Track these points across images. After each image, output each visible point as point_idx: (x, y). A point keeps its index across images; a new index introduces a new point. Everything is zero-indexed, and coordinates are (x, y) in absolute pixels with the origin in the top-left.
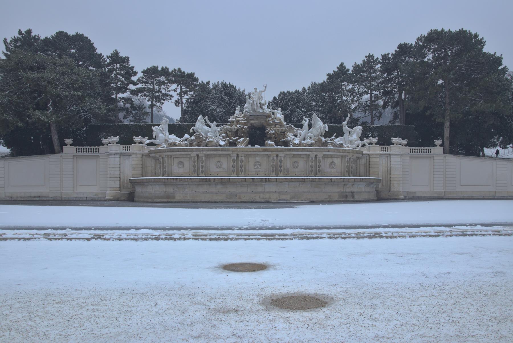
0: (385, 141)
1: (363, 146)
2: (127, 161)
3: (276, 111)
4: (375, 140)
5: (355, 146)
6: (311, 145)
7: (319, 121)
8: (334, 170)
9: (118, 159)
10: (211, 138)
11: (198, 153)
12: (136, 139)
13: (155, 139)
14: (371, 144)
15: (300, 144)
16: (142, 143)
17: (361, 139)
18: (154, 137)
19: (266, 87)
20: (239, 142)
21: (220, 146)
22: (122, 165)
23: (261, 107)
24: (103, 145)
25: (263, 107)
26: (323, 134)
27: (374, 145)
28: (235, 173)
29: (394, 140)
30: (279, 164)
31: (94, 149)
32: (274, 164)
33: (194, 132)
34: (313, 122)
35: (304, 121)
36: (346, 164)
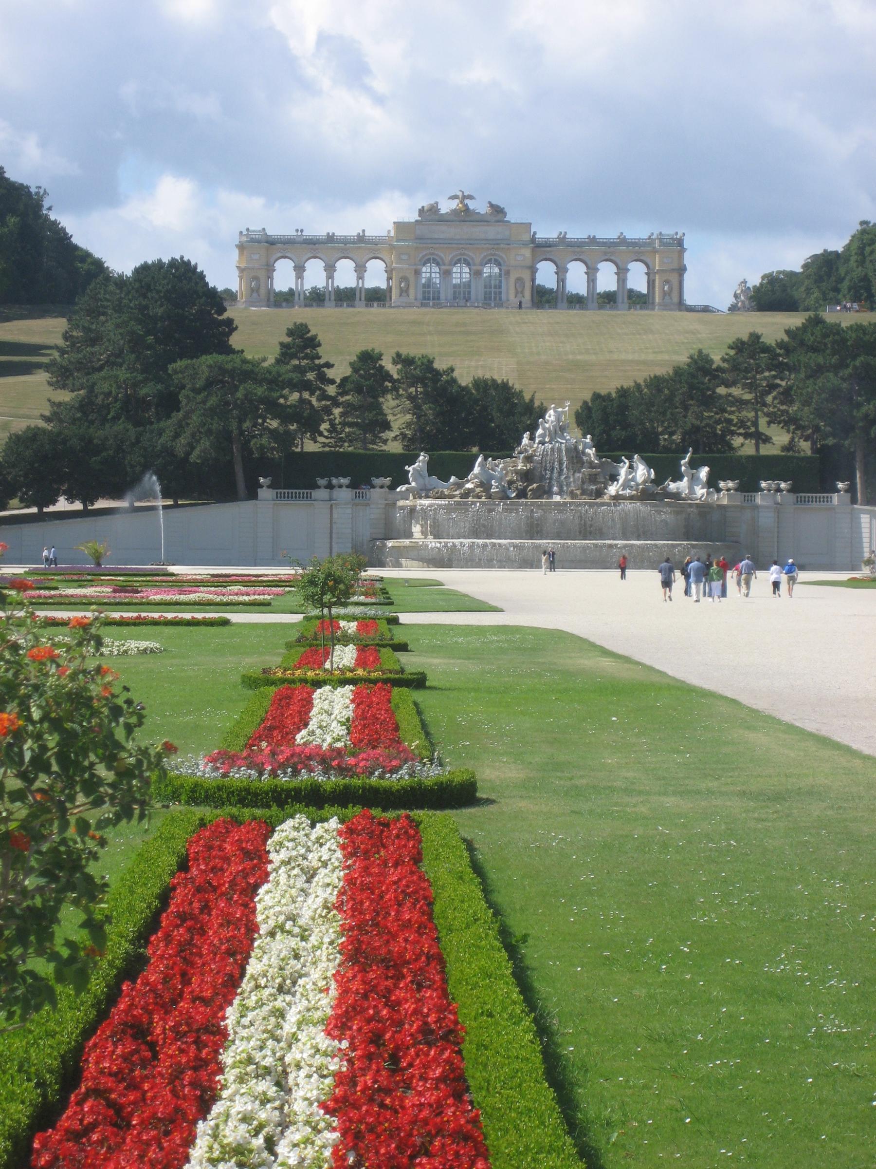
0: (749, 487)
6: (631, 498)
9: (349, 511)
12: (377, 481)
17: (712, 483)
20: (530, 490)
24: (319, 487)
29: (763, 484)
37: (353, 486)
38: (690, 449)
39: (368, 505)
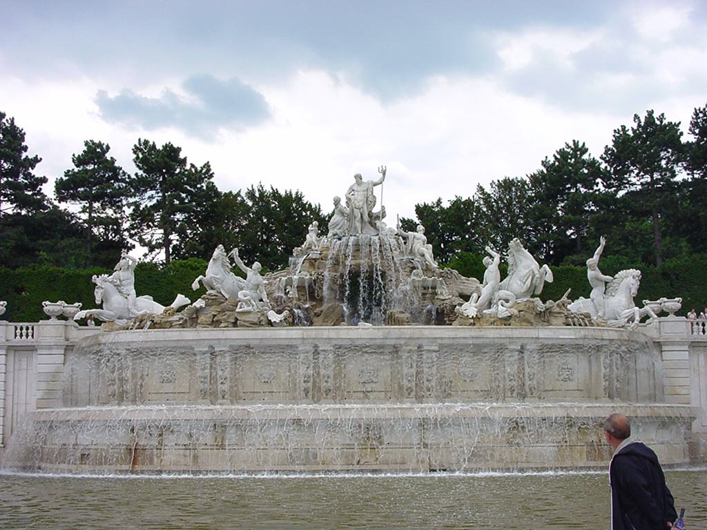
1: (644, 319)
2: (24, 364)
4: (675, 303)
5: (623, 321)
6: (507, 321)
7: (526, 257)
10: (248, 303)
12: (48, 306)
13: (100, 307)
14: (663, 314)
15: (477, 319)
16: (66, 319)
17: (638, 301)
18: (98, 302)
19: (384, 174)
21: (270, 323)
22: (11, 375)
23: (374, 225)
25: (378, 223)
26: (539, 291)
27: (671, 317)
33: (202, 291)
34: (510, 259)
35: (486, 260)
36: (604, 371)
38: (603, 241)
39: (32, 349)
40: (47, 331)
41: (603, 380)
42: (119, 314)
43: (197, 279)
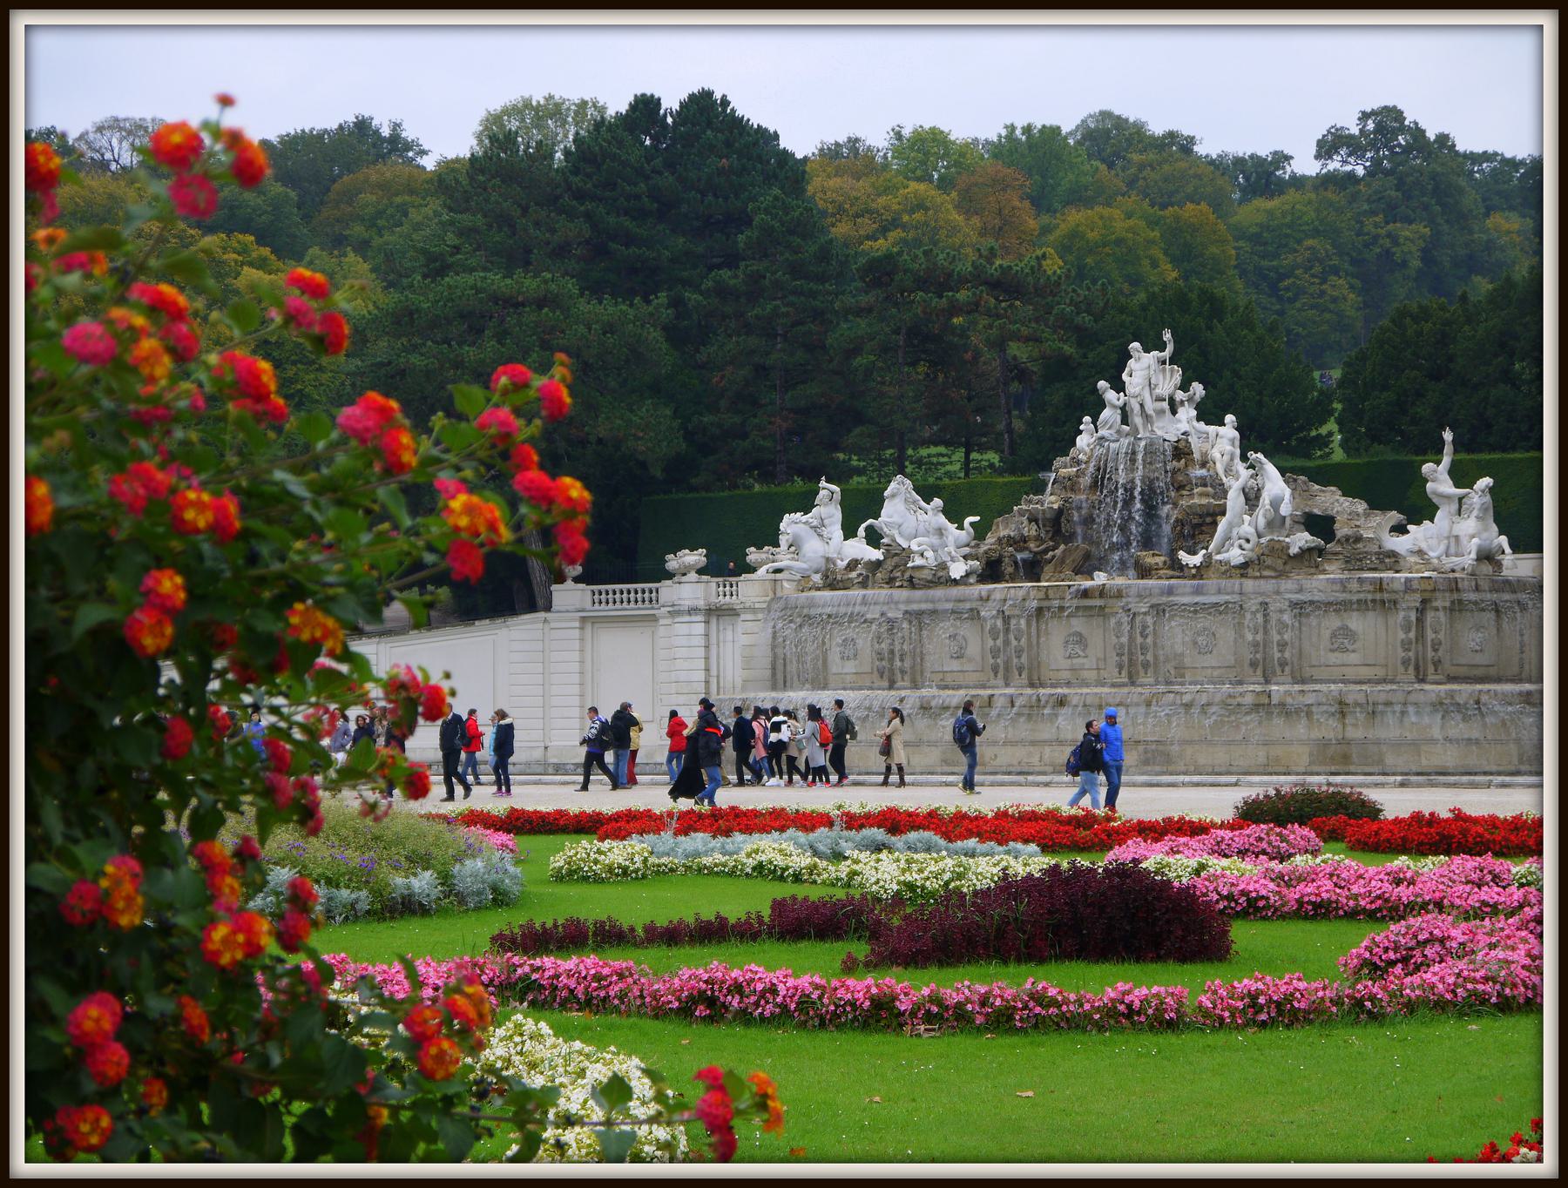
3: (1212, 429)
8: (1353, 658)
11: (885, 608)
21: (955, 582)
24: (669, 576)
28: (1000, 675)
30: (1139, 640)
31: (643, 592)
32: (1124, 640)
37: (709, 570)
38: (1448, 436)
40: (750, 589)
41: (1400, 650)
42: (815, 566)
43: (864, 525)
